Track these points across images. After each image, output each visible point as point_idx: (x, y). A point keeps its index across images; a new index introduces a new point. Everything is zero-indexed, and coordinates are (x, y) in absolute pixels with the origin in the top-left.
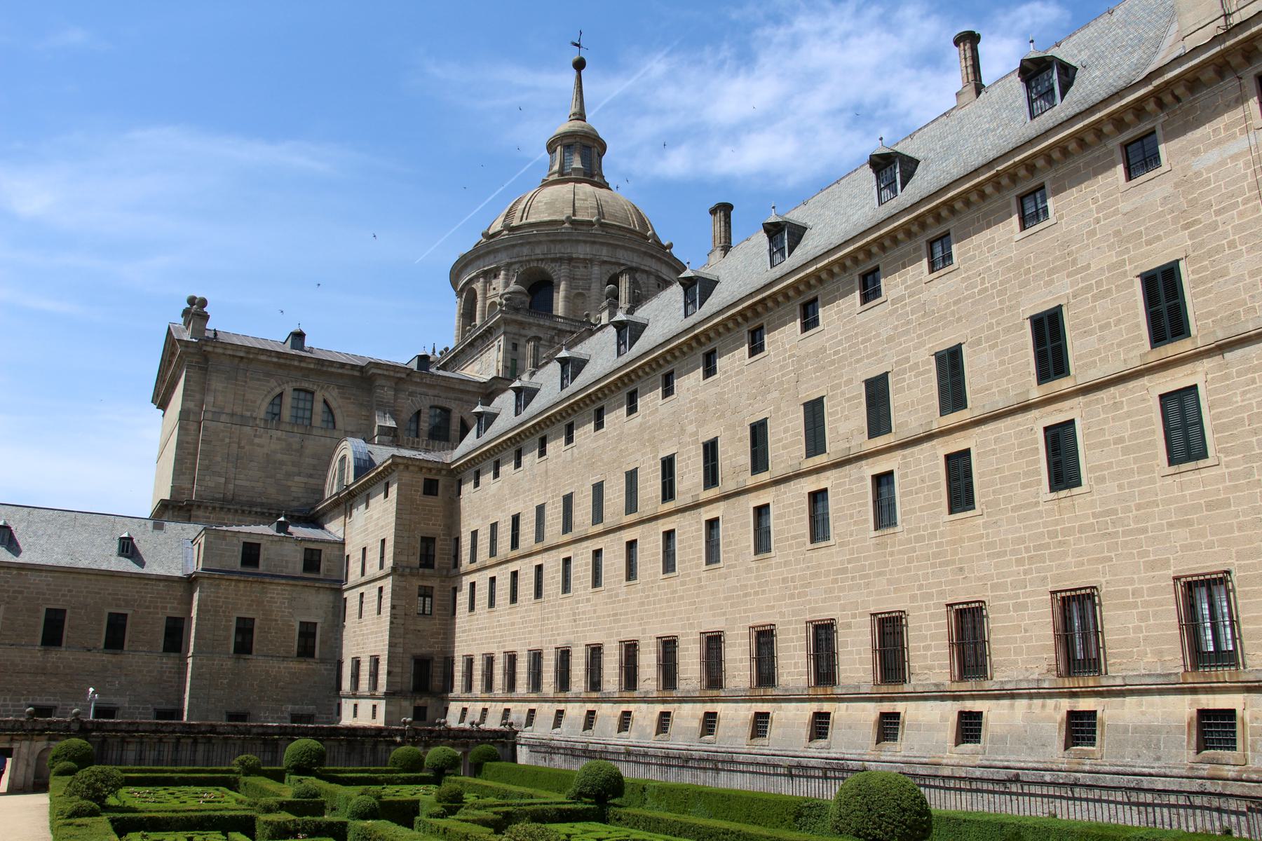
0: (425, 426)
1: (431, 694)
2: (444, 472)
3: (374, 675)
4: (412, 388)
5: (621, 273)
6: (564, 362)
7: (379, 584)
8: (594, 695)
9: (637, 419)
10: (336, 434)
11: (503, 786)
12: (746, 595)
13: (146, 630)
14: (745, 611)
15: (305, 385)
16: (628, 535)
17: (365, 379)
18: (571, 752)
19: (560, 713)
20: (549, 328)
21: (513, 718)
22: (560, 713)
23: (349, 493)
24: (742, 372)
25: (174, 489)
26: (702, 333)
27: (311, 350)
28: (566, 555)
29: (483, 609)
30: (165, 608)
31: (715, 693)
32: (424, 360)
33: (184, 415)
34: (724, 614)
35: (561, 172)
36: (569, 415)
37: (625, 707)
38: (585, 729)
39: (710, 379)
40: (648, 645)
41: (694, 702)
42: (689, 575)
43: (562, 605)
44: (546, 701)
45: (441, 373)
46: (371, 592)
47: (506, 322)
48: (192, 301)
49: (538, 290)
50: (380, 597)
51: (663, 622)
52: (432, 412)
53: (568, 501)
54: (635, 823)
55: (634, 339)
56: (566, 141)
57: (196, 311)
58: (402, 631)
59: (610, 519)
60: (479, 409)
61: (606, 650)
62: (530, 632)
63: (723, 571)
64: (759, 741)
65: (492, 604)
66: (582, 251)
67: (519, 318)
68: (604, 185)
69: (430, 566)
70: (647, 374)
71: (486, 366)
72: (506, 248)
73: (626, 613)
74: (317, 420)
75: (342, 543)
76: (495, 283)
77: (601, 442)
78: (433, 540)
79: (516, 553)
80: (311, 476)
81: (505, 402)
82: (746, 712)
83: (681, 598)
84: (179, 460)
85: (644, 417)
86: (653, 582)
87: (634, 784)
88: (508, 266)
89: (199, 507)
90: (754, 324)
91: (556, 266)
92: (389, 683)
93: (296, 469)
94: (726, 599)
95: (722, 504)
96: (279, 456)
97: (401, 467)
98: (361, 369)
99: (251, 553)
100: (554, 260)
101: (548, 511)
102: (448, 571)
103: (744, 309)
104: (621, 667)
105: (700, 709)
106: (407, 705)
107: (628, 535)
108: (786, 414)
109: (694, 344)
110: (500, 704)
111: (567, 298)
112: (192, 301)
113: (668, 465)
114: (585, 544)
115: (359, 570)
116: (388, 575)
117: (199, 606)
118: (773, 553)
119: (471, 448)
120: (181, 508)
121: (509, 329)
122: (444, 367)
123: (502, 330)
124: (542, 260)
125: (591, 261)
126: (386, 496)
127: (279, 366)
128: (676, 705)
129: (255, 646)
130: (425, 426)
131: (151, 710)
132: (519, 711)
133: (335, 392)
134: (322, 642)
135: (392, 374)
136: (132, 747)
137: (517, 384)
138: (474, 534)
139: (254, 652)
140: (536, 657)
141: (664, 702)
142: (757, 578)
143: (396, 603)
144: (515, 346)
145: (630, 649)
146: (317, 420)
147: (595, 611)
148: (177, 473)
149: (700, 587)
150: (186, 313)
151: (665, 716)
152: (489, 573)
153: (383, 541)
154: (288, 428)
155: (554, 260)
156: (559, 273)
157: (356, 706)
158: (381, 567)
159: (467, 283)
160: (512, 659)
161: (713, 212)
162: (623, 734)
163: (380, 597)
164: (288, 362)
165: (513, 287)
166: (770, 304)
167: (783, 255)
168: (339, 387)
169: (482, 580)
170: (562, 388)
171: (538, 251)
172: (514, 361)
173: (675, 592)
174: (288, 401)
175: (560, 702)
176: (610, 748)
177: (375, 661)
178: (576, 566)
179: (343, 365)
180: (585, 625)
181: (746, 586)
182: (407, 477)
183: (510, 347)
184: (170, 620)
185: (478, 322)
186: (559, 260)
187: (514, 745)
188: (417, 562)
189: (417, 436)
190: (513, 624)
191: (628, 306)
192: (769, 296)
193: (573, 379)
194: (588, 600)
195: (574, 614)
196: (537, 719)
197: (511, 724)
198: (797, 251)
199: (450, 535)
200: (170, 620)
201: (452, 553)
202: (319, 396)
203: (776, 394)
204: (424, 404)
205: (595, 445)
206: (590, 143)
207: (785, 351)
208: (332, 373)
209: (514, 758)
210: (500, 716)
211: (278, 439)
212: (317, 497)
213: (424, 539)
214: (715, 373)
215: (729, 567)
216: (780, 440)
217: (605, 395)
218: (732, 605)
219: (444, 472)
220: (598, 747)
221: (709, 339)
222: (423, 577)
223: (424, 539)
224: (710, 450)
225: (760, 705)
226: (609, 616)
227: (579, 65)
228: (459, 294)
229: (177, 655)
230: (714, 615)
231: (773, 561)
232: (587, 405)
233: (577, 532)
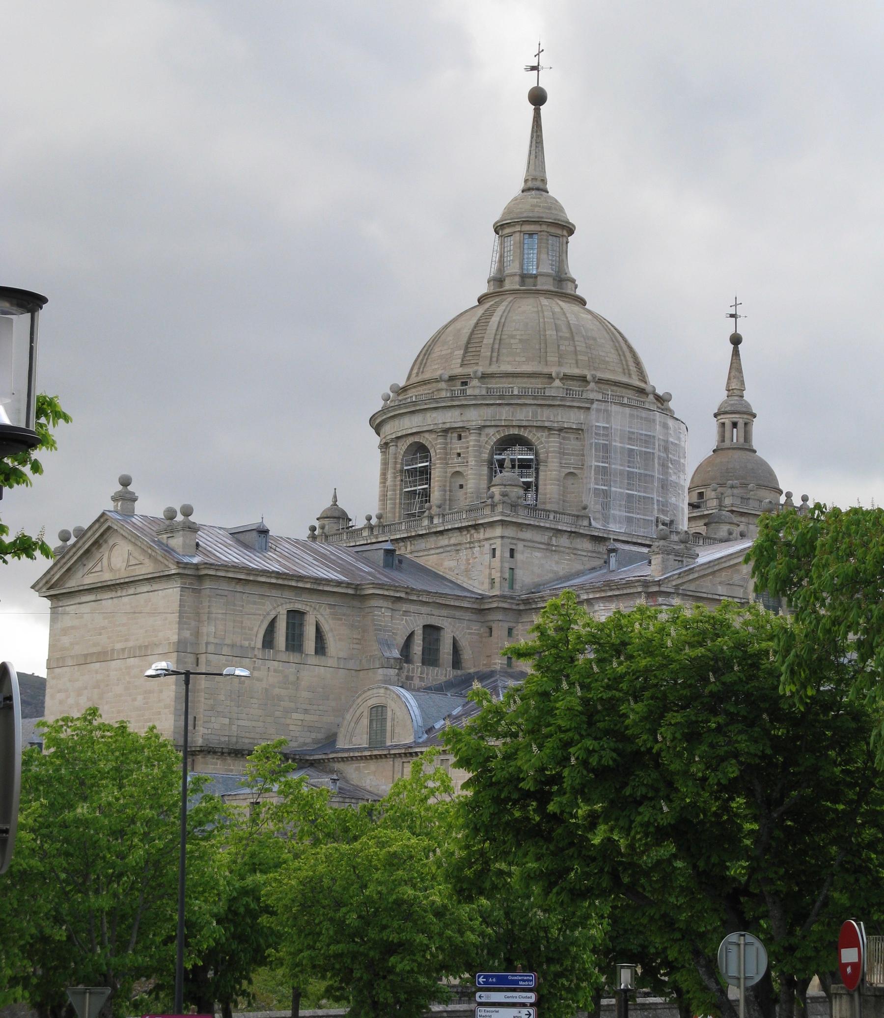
10: (330, 662)
15: (298, 606)
74: (310, 644)
76: (457, 446)
80: (306, 711)
124: (525, 427)
146: (310, 644)
154: (284, 656)
204: (416, 623)
211: (275, 671)
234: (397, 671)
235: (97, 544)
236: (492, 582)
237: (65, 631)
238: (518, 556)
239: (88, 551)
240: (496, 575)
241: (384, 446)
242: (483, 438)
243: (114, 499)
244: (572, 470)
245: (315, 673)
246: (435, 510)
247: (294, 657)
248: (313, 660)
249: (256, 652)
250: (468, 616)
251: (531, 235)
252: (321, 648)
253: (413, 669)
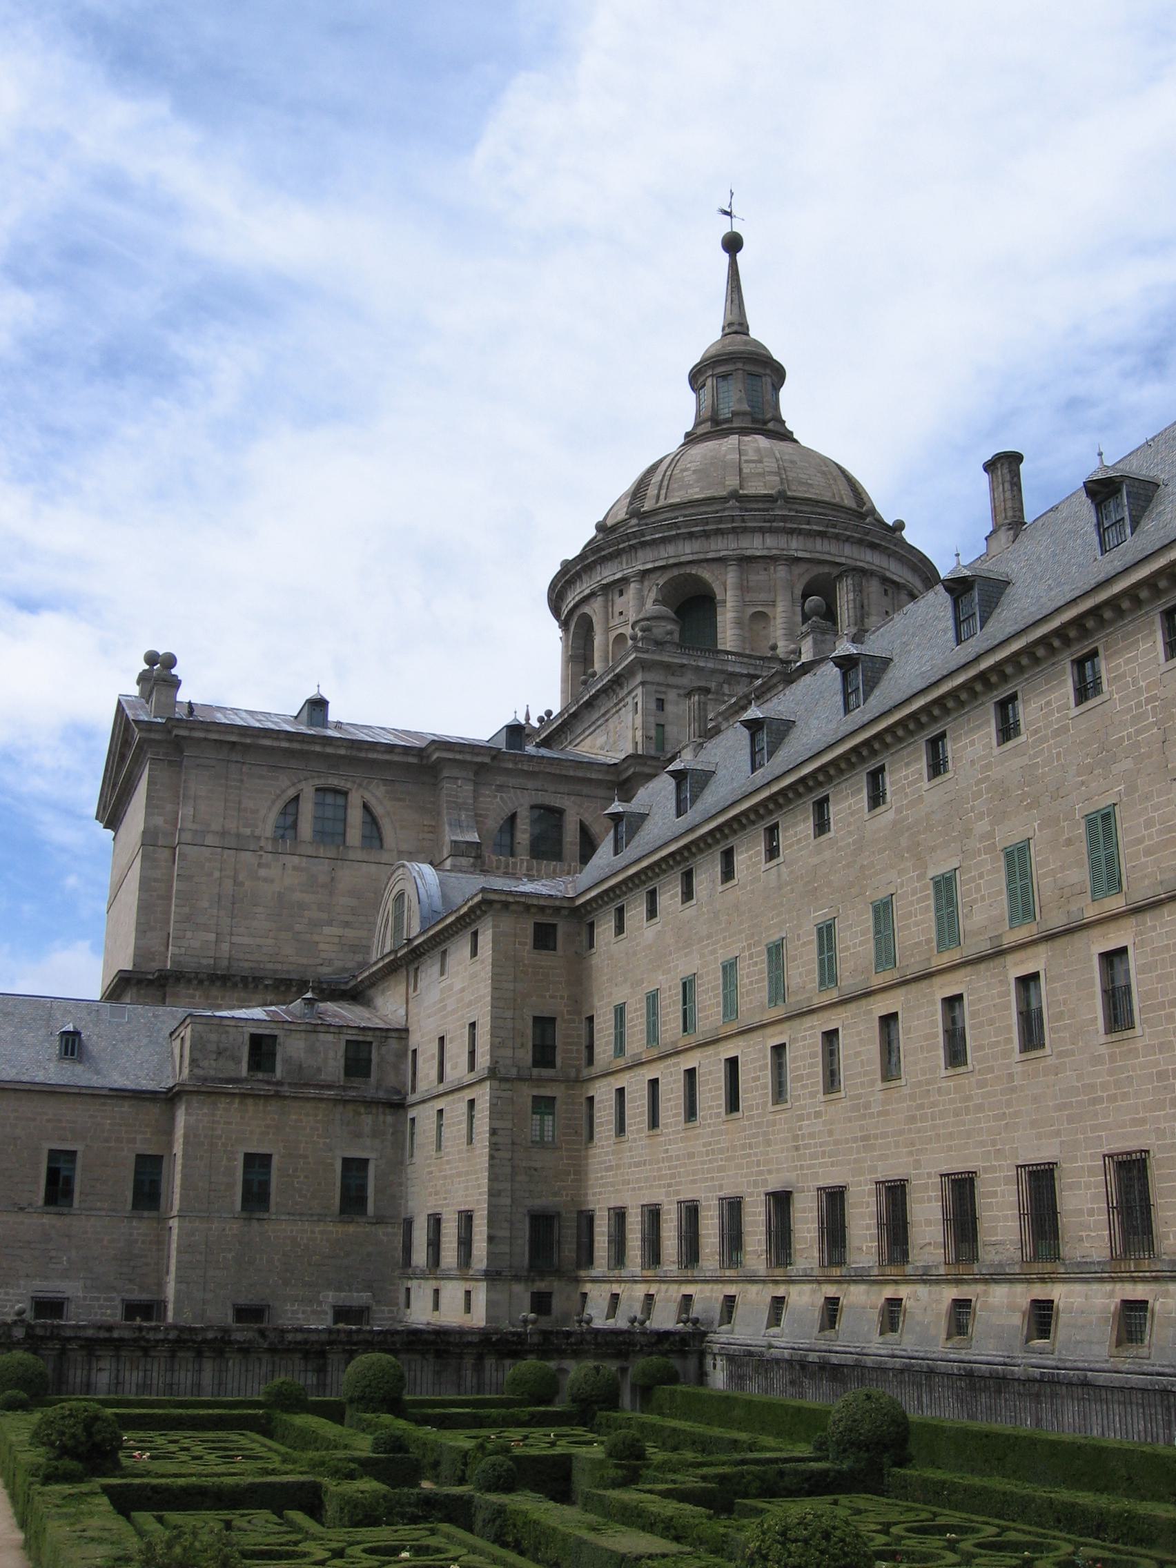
0: (523, 836)
1: (558, 1273)
2: (565, 912)
3: (465, 1243)
4: (500, 780)
5: (839, 577)
6: (754, 726)
7: (468, 1095)
8: (836, 1272)
9: (886, 815)
10: (385, 857)
11: (700, 1429)
12: (1094, 1101)
13: (105, 1177)
14: (1094, 1128)
15: (334, 782)
16: (882, 1006)
17: (425, 765)
18: (803, 1368)
19: (778, 1302)
20: (713, 671)
21: (696, 1311)
22: (778, 1302)
23: (413, 951)
24: (1064, 729)
25: (141, 953)
26: (991, 669)
27: (339, 725)
28: (777, 1041)
29: (639, 1131)
30: (133, 1141)
31: (1049, 1267)
32: (515, 732)
33: (150, 839)
34: (1058, 1133)
36: (770, 812)
37: (889, 1292)
38: (822, 1329)
39: (1010, 744)
40: (925, 1187)
41: (1010, 1281)
42: (991, 1070)
43: (774, 1123)
44: (752, 1280)
45: (544, 752)
46: (456, 1108)
48: (152, 658)
49: (691, 605)
50: (471, 1118)
51: (950, 1148)
52: (537, 812)
53: (776, 952)
54: (937, 1494)
55: (871, 684)
56: (721, 370)
57: (160, 673)
58: (509, 1170)
59: (848, 979)
60: (617, 807)
61: (851, 1198)
62: (721, 1169)
63: (1050, 1061)
64: (1133, 1350)
65: (654, 1122)
67: (666, 659)
68: (787, 436)
69: (545, 1060)
70: (900, 740)
71: (613, 739)
73: (884, 1135)
74: (354, 835)
75: (403, 1033)
77: (827, 854)
78: (552, 1020)
79: (692, 1040)
80: (347, 924)
81: (657, 795)
82: (1103, 1299)
83: (980, 1108)
84: (144, 908)
85: (899, 811)
86: (928, 1083)
87: (924, 1426)
88: (645, 574)
89: (178, 980)
90: (1080, 650)
92: (491, 1255)
93: (324, 916)
94: (1060, 1108)
95: (1042, 949)
96: (298, 896)
97: (498, 906)
98: (420, 752)
99: (262, 1048)
101: (743, 970)
102: (578, 1071)
103: (1065, 626)
104: (880, 1225)
105: (1023, 1295)
106: (522, 1293)
107: (882, 1006)
108: (1147, 797)
109: (979, 687)
110: (674, 1287)
111: (739, 623)
112: (152, 658)
113: (945, 887)
114: (808, 1021)
115: (434, 1073)
116: (482, 1080)
117: (186, 1136)
118: (1138, 1030)
119: (607, 871)
120: (151, 982)
121: (650, 677)
122: (546, 743)
123: (639, 678)
126: (474, 953)
128: (980, 1288)
129: (274, 1198)
130: (523, 836)
131: (117, 1302)
132: (707, 1297)
133: (380, 791)
134: (376, 1192)
135: (468, 758)
136: (102, 1364)
137: (676, 766)
138: (620, 1011)
139: (273, 1209)
140: (733, 1208)
141: (958, 1282)
142: (1111, 1072)
143: (498, 1124)
144: (661, 704)
145: (895, 1195)
146: (354, 835)
147: (830, 1133)
148: (142, 929)
149: (1013, 1090)
150: (143, 679)
151: (962, 1306)
152: (649, 1073)
153: (473, 1025)
154: (310, 850)
157: (437, 1292)
158: (472, 1067)
159: (576, 606)
160: (691, 1212)
161: (989, 467)
162: (891, 1336)
163: (471, 1118)
164: (306, 747)
165: (650, 608)
166: (1108, 614)
167: (1121, 532)
168: (385, 781)
169: (636, 1084)
170: (753, 769)
172: (660, 726)
173: (968, 1098)
174: (307, 809)
175: (776, 1282)
176: (869, 1361)
177: (467, 1218)
178: (794, 1059)
179: (391, 748)
180: (814, 1156)
181: (1092, 1086)
182: (507, 923)
183: (653, 706)
184: (141, 1159)
185: (598, 666)
187: (702, 1355)
188: (529, 1058)
189: (512, 855)
190: (691, 1155)
191: (853, 630)
192: (1107, 603)
193: (771, 754)
194: (818, 1115)
195: (796, 1138)
196: (739, 1312)
197: (696, 1321)
198: (1147, 525)
199: (579, 1013)
200: (141, 1159)
201: (584, 1042)
202: (355, 799)
203: (1127, 764)
204: (521, 801)
205: (815, 860)
206: (760, 370)
207: (1139, 691)
208: (374, 761)
209: (702, 1377)
210: (674, 1307)
211: (295, 868)
212: (359, 958)
213: (536, 1019)
214: (1018, 734)
215: (1060, 1055)
216: (1140, 841)
217: (830, 779)
218: (1070, 1119)
219: (565, 912)
220: (849, 1359)
221: (1005, 678)
222: (540, 1081)
223: (536, 1019)
224: (1017, 860)
225: (1128, 1287)
226: (855, 1140)
227: (733, 244)
228: (564, 625)
229: (154, 1214)
230: (1039, 1137)
231: (1140, 1044)
232: (800, 795)
233: (795, 1000)
234: (472, 860)
238: (669, 708)
244: (760, 609)
249: (262, 843)
253: (515, 864)
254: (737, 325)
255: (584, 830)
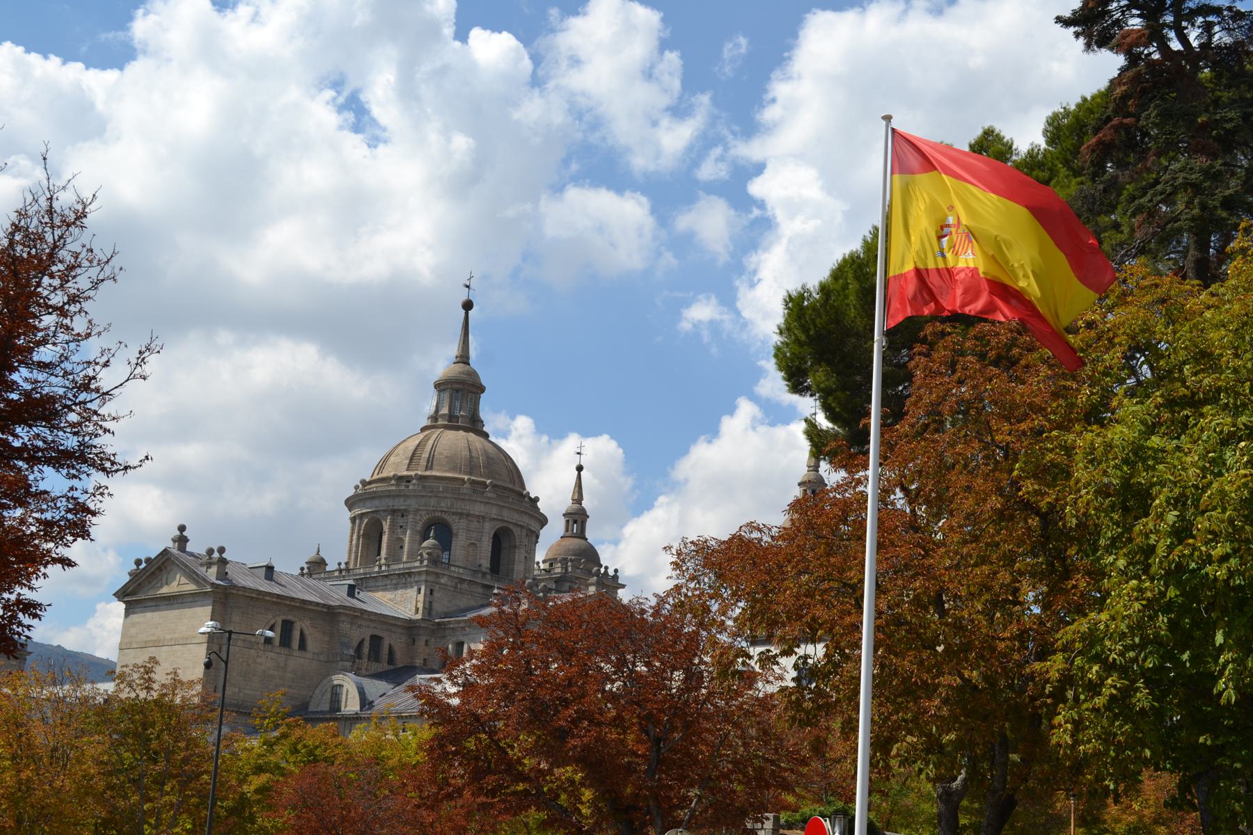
10: (308, 655)
15: (290, 617)
35: (451, 417)
47: (427, 573)
56: (455, 386)
66: (478, 509)
68: (486, 436)
72: (415, 496)
74: (295, 643)
76: (401, 521)
91: (456, 518)
100: (454, 514)
121: (430, 578)
123: (423, 577)
125: (483, 517)
127: (275, 603)
133: (308, 623)
146: (295, 643)
154: (278, 650)
155: (454, 514)
156: (458, 525)
171: (443, 504)
186: (461, 515)
204: (367, 633)
235: (160, 569)
236: (417, 609)
237: (133, 625)
238: (435, 594)
239: (153, 573)
240: (420, 606)
241: (353, 520)
242: (418, 517)
243: (174, 541)
245: (297, 661)
246: (383, 561)
247: (284, 651)
248: (296, 653)
250: (400, 631)
251: (457, 391)
252: (303, 646)
254: (464, 358)
255: (390, 647)
